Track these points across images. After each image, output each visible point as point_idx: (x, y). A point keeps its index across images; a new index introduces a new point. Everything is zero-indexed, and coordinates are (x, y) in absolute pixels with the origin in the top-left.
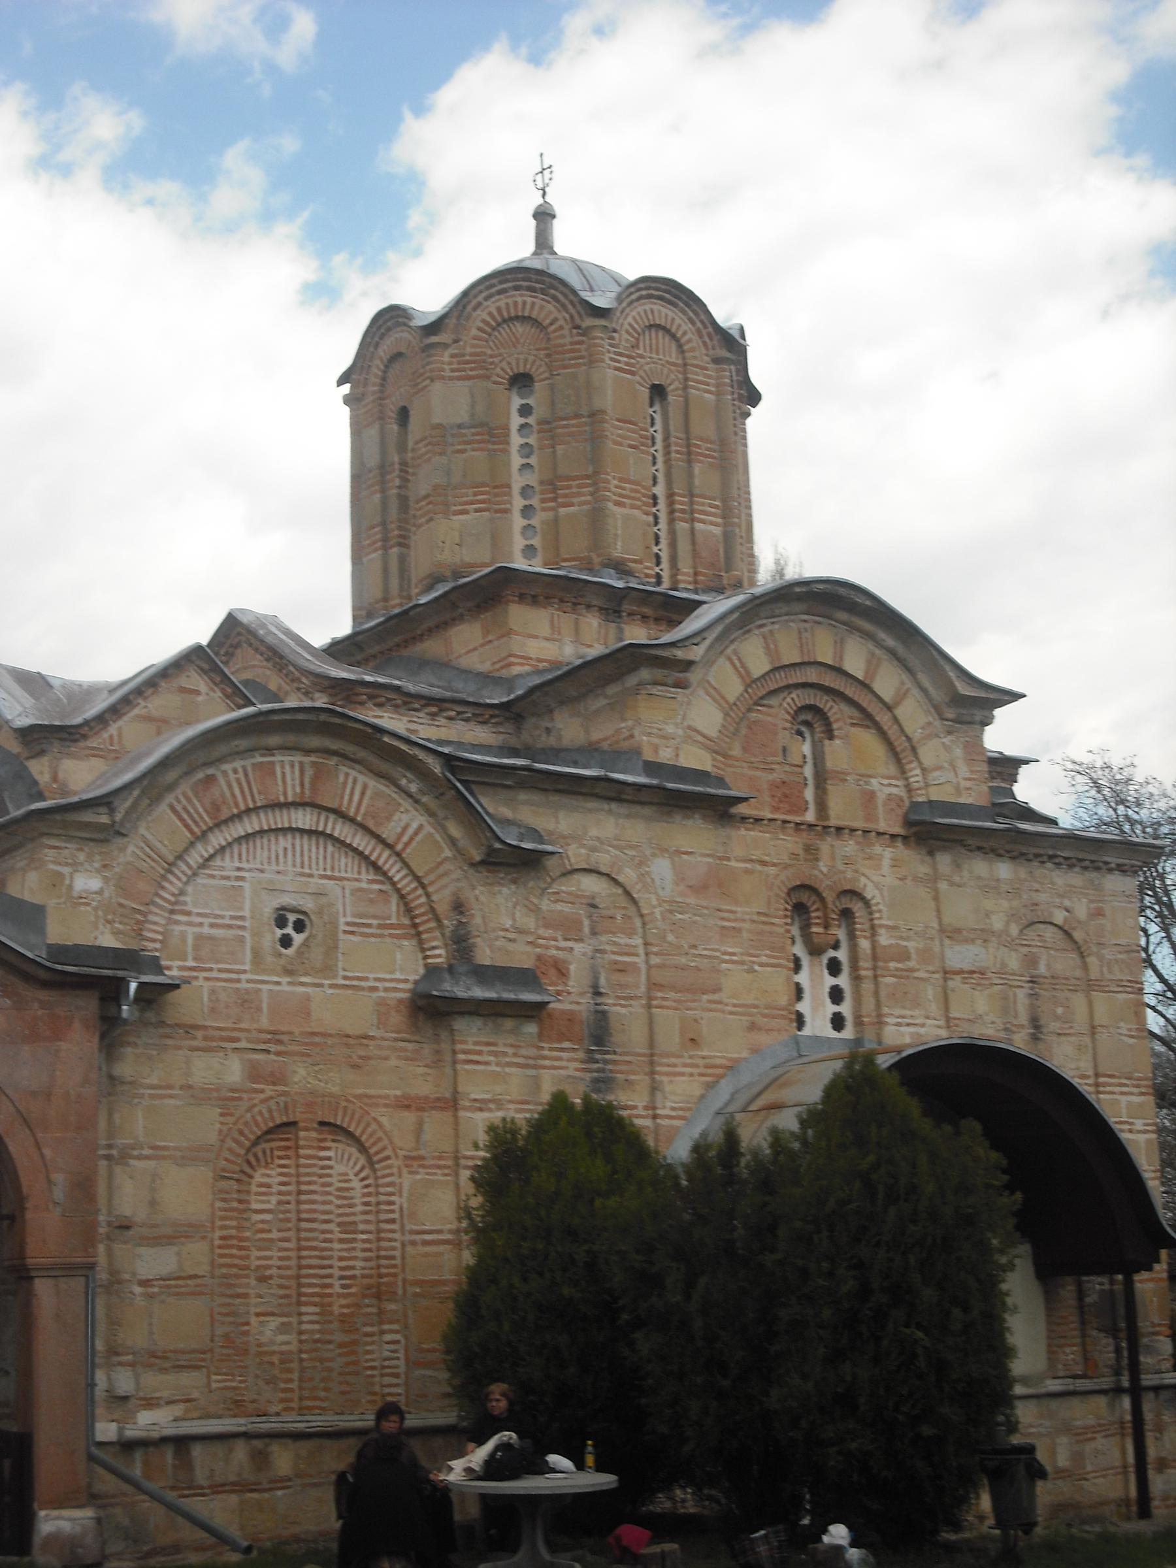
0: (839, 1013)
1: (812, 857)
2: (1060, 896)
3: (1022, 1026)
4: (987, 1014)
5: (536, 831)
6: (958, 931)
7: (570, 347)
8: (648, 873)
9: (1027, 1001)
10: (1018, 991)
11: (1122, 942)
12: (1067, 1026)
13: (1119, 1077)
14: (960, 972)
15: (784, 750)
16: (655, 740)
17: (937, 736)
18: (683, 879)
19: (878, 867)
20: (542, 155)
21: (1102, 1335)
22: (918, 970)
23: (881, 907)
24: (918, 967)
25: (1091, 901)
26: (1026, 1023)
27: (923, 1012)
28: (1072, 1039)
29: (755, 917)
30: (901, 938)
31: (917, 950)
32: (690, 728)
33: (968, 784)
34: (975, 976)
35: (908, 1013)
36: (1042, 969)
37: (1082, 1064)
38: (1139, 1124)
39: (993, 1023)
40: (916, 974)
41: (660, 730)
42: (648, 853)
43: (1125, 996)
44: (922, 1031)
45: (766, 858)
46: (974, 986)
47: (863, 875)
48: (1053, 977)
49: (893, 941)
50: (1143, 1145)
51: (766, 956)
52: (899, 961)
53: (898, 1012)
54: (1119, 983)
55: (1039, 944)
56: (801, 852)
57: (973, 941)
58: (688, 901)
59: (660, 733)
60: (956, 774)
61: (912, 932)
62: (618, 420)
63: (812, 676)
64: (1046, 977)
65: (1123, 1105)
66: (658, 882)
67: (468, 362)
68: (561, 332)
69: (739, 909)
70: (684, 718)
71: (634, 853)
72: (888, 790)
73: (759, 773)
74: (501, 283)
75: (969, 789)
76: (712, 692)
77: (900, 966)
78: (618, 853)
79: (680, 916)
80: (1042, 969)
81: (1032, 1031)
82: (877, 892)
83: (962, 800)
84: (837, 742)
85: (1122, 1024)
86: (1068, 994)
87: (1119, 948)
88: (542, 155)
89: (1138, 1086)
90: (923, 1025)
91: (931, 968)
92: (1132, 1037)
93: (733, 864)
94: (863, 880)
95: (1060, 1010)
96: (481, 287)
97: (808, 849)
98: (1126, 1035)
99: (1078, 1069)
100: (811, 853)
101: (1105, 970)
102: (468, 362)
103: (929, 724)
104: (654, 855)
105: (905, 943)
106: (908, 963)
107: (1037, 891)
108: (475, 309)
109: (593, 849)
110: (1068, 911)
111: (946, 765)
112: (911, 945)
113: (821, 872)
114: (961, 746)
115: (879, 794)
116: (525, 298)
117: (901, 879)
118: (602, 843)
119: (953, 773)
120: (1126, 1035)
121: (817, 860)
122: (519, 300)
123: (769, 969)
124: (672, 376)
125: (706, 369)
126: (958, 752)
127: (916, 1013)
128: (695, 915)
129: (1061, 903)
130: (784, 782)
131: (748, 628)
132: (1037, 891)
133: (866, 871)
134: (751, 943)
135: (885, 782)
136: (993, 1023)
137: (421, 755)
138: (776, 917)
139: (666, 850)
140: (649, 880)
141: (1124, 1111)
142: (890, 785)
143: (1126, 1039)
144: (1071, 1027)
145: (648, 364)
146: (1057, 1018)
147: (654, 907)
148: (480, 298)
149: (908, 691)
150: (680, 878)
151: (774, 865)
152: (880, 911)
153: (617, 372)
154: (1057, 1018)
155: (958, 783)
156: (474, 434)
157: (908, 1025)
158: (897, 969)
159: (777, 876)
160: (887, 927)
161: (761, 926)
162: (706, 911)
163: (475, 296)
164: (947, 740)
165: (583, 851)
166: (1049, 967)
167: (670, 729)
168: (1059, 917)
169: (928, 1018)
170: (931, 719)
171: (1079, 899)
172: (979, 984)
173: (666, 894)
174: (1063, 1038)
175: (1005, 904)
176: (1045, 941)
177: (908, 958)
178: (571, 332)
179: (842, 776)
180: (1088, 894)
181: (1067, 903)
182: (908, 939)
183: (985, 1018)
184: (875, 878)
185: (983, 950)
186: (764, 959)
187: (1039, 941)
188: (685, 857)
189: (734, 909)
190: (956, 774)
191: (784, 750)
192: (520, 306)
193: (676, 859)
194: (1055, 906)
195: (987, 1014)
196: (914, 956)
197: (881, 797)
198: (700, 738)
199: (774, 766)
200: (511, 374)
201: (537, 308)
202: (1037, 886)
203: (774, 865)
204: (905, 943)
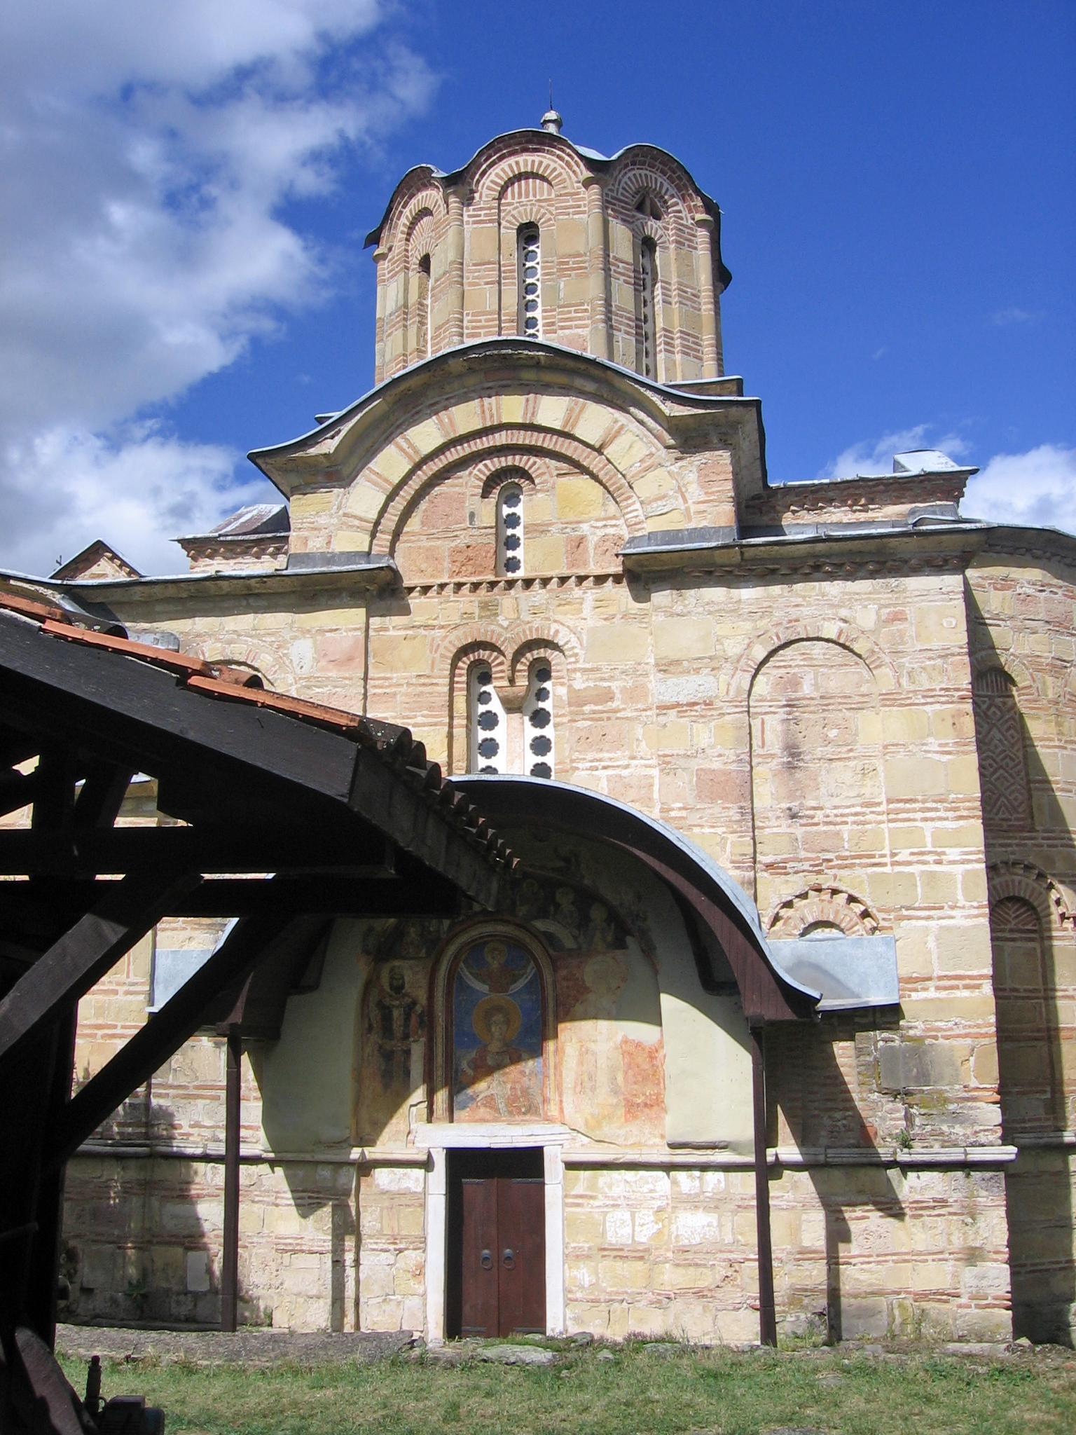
0: (543, 764)
1: (488, 613)
2: (832, 606)
3: (772, 756)
4: (712, 747)
5: (172, 634)
6: (678, 662)
8: (285, 655)
9: (779, 728)
10: (766, 717)
11: (935, 645)
12: (845, 749)
13: (924, 802)
14: (678, 705)
15: (472, 515)
16: (306, 534)
17: (660, 465)
18: (325, 655)
19: (580, 611)
21: (885, 1099)
22: (624, 709)
23: (576, 651)
24: (621, 707)
25: (882, 606)
26: (778, 752)
27: (627, 753)
28: (852, 764)
29: (414, 681)
30: (602, 679)
31: (623, 690)
32: (345, 515)
33: (702, 507)
34: (696, 708)
35: (606, 755)
36: (807, 689)
37: (867, 791)
38: (953, 853)
39: (720, 755)
40: (619, 715)
41: (313, 523)
42: (287, 637)
43: (937, 707)
44: (625, 773)
45: (430, 622)
46: (694, 719)
47: (555, 621)
48: (822, 697)
49: (591, 684)
50: (959, 878)
51: (423, 716)
52: (596, 704)
53: (590, 756)
54: (928, 694)
55: (802, 663)
56: (477, 611)
57: (697, 671)
58: (330, 674)
59: (312, 526)
60: (685, 501)
61: (617, 672)
62: (474, 265)
63: (501, 439)
64: (812, 699)
65: (928, 834)
66: (296, 661)
69: (395, 675)
70: (339, 508)
71: (273, 639)
72: (600, 533)
73: (439, 542)
75: (699, 512)
76: (374, 477)
77: (599, 708)
78: (256, 641)
79: (317, 690)
80: (807, 689)
81: (785, 760)
82: (574, 639)
83: (692, 525)
84: (540, 495)
85: (931, 740)
86: (848, 714)
87: (930, 654)
89: (955, 809)
90: (627, 767)
91: (640, 706)
92: (949, 753)
93: (391, 633)
94: (554, 627)
95: (833, 733)
97: (484, 606)
98: (937, 752)
99: (858, 796)
100: (489, 609)
101: (904, 681)
103: (651, 455)
104: (294, 638)
105: (606, 684)
106: (610, 703)
107: (797, 606)
108: (399, 219)
109: (230, 642)
110: (845, 621)
111: (671, 493)
112: (615, 686)
113: (501, 626)
114: (695, 469)
115: (590, 538)
117: (606, 619)
118: (239, 635)
119: (680, 500)
120: (937, 752)
121: (496, 615)
123: (426, 729)
124: (543, 211)
125: (578, 194)
126: (692, 476)
127: (619, 753)
128: (335, 687)
129: (836, 614)
130: (468, 547)
131: (418, 409)
132: (797, 606)
133: (558, 617)
134: (407, 706)
135: (600, 524)
136: (720, 755)
137: (41, 590)
138: (440, 677)
139: (309, 631)
140: (287, 662)
141: (929, 840)
142: (605, 526)
143: (937, 757)
144: (851, 750)
145: (514, 209)
146: (827, 742)
147: (291, 685)
149: (622, 427)
150: (321, 654)
151: (442, 627)
152: (576, 655)
153: (475, 226)
154: (827, 742)
155: (687, 509)
157: (605, 768)
158: (594, 712)
159: (446, 637)
160: (585, 670)
161: (421, 689)
162: (347, 682)
164: (674, 468)
165: (219, 645)
166: (816, 686)
167: (323, 520)
168: (830, 630)
169: (633, 758)
170: (653, 450)
171: (866, 607)
172: (703, 716)
173: (306, 671)
174: (834, 764)
175: (748, 626)
176: (812, 659)
177: (612, 699)
179: (542, 528)
180: (879, 599)
181: (844, 613)
182: (612, 678)
183: (708, 751)
184: (571, 623)
185: (711, 678)
186: (419, 720)
187: (804, 659)
188: (328, 634)
189: (388, 675)
190: (685, 501)
191: (472, 515)
193: (319, 638)
194: (824, 619)
195: (712, 747)
196: (618, 695)
197: (592, 541)
198: (357, 522)
199: (458, 533)
202: (799, 600)
203: (442, 627)
204: (606, 684)
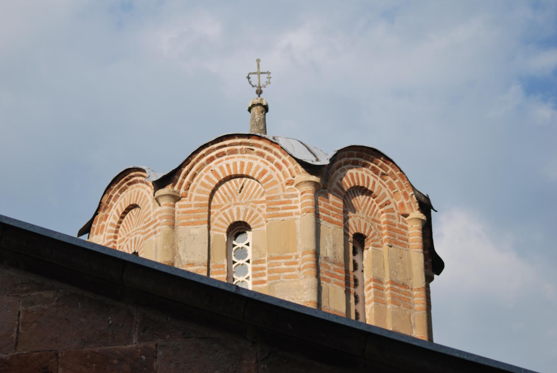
7: (398, 228)
20: (258, 61)
67: (331, 209)
68: (393, 214)
74: (358, 156)
88: (258, 61)
96: (346, 153)
102: (331, 209)
116: (370, 176)
122: (366, 175)
148: (343, 161)
156: (335, 270)
163: (340, 159)
178: (399, 217)
192: (366, 181)
200: (356, 232)
201: (376, 186)
